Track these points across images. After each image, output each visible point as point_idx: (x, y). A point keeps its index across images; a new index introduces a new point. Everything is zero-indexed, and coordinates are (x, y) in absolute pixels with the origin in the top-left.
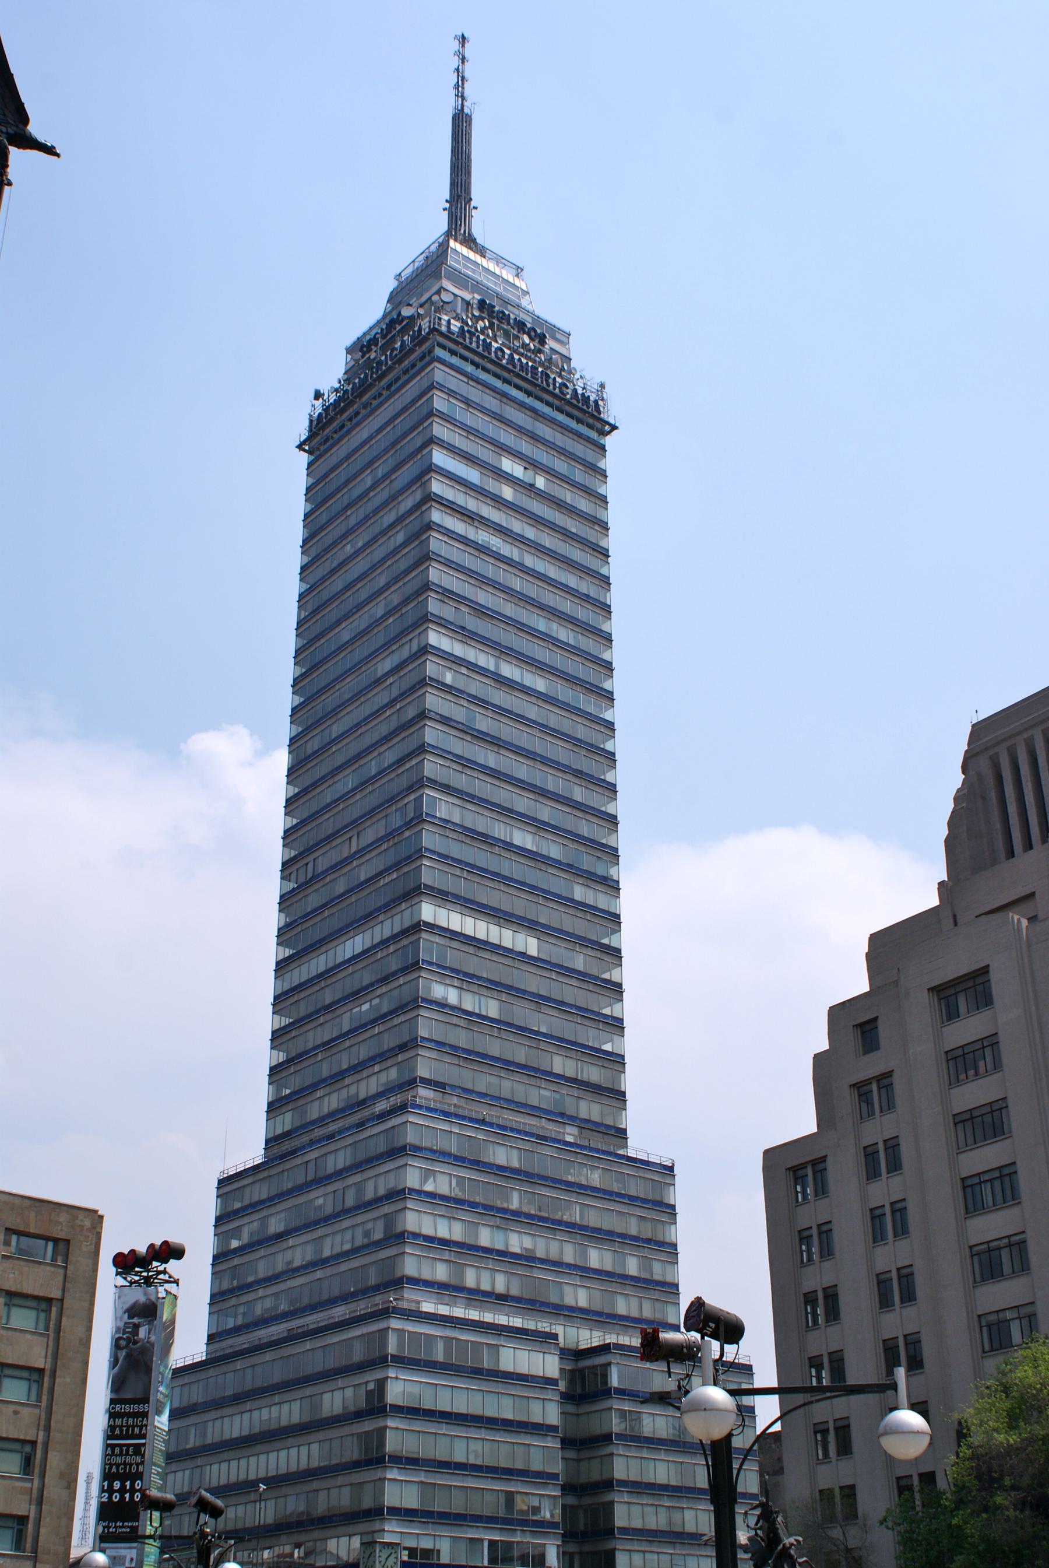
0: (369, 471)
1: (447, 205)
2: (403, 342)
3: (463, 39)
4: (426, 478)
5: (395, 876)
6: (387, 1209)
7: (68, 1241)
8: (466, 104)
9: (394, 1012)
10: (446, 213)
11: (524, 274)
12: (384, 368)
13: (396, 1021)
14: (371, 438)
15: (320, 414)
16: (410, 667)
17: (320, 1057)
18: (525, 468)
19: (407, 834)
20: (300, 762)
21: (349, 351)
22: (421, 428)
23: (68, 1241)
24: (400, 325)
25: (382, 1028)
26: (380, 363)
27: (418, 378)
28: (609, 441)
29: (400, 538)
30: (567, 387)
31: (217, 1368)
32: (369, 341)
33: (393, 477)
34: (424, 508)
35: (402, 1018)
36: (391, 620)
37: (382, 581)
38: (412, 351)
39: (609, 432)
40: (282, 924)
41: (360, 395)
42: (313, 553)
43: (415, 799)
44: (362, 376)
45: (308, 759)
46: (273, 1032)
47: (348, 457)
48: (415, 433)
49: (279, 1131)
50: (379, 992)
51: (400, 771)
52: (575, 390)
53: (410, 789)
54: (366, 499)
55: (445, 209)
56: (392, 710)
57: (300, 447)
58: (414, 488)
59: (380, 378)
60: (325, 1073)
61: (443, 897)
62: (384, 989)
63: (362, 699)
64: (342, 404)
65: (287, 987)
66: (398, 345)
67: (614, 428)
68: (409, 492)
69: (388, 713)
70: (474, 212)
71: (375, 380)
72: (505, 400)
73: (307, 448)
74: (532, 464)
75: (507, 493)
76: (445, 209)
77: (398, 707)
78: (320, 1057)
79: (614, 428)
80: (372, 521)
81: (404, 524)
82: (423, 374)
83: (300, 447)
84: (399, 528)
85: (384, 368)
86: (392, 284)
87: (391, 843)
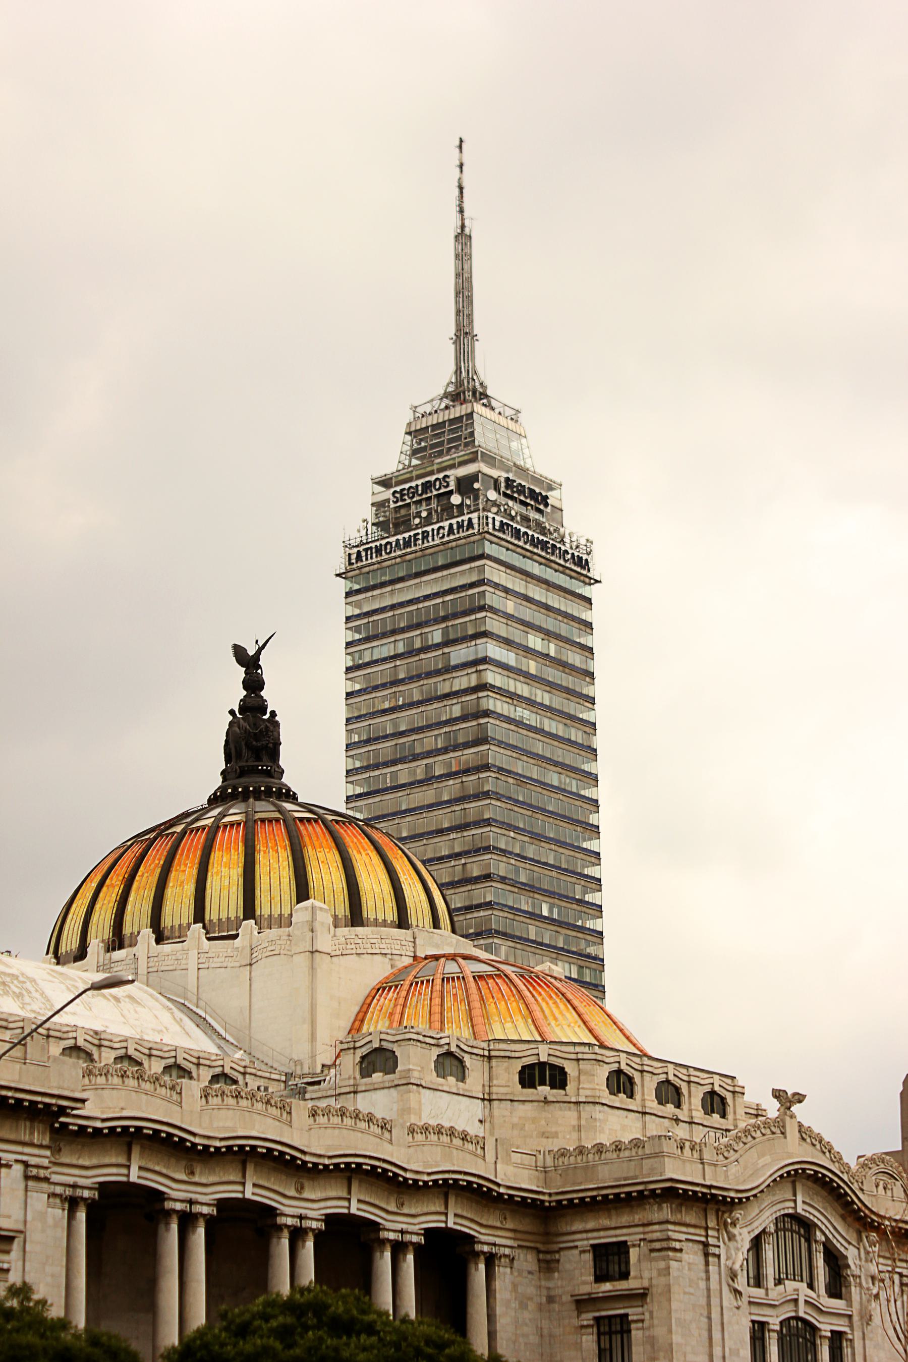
8: (467, 223)
11: (522, 418)
18: (543, 640)
29: (457, 711)
30: (568, 553)
33: (446, 650)
36: (451, 782)
39: (593, 584)
47: (393, 607)
48: (467, 619)
51: (469, 916)
52: (573, 554)
56: (457, 863)
58: (470, 671)
68: (465, 672)
70: (476, 343)
72: (529, 579)
74: (548, 634)
75: (532, 667)
77: (463, 861)
81: (460, 701)
83: (337, 575)
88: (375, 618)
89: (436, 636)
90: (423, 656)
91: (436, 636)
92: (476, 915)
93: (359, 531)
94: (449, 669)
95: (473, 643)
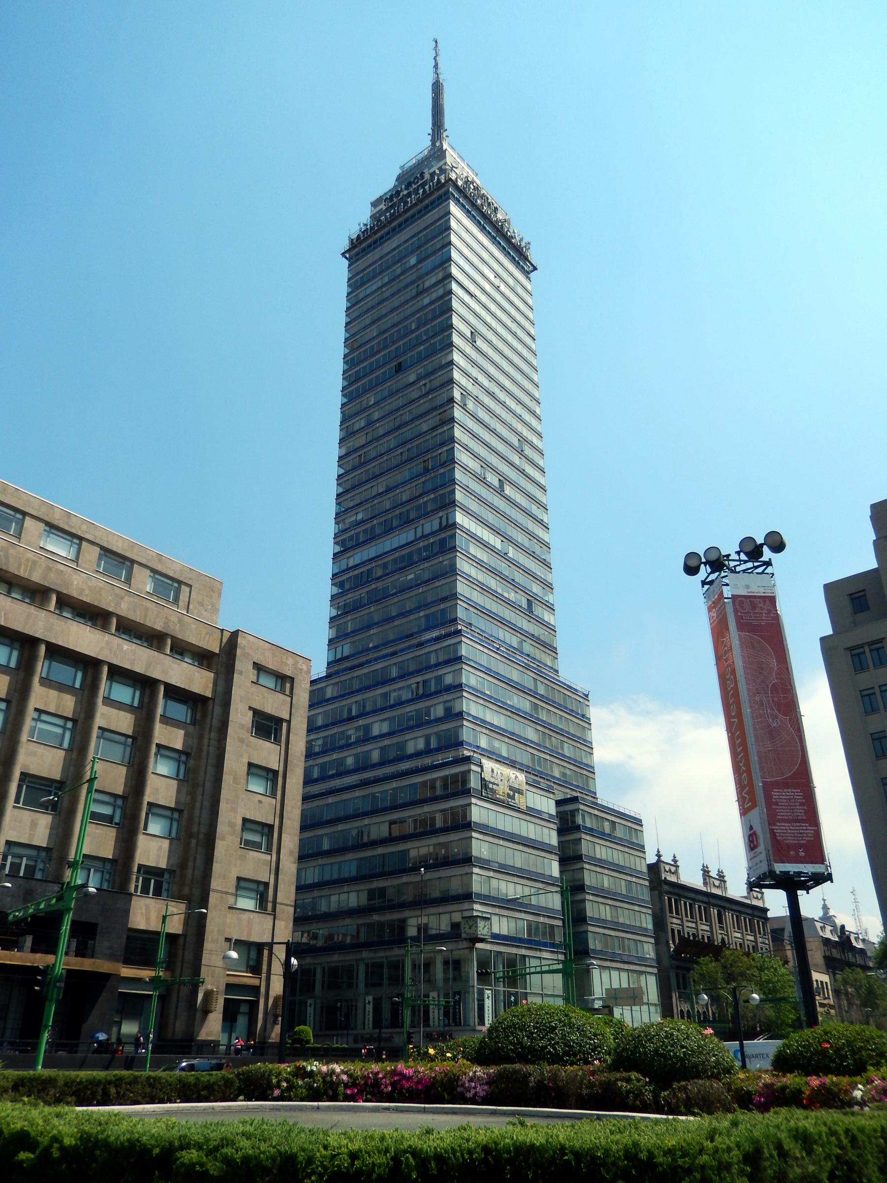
0: (399, 264)
1: (430, 132)
2: (424, 191)
3: (436, 42)
4: (446, 265)
5: (432, 496)
6: (446, 697)
7: (292, 680)
9: (435, 578)
10: (430, 137)
12: (409, 205)
13: (437, 584)
14: (399, 246)
15: (358, 235)
16: (439, 374)
17: (372, 609)
19: (442, 471)
20: (351, 434)
21: (374, 204)
22: (441, 237)
23: (292, 680)
24: (415, 184)
25: (425, 589)
26: (406, 203)
27: (437, 209)
28: (532, 275)
31: (310, 803)
32: (391, 196)
33: (419, 266)
34: (446, 282)
35: (443, 582)
37: (413, 327)
38: (431, 193)
40: (337, 531)
41: (390, 223)
42: (354, 315)
43: (447, 450)
44: (392, 211)
45: (354, 433)
46: (332, 596)
47: (381, 258)
49: (339, 656)
50: (422, 567)
51: (434, 434)
53: (442, 444)
54: (398, 281)
55: (429, 134)
56: (425, 400)
57: (343, 254)
58: (437, 271)
59: (405, 212)
60: (376, 618)
61: (467, 512)
62: (426, 565)
63: (400, 395)
64: (376, 228)
65: (344, 567)
66: (421, 191)
67: (535, 269)
68: (434, 273)
69: (422, 401)
71: (403, 212)
73: (348, 256)
76: (429, 134)
77: (430, 397)
78: (372, 609)
79: (535, 269)
80: (403, 292)
82: (440, 207)
83: (343, 254)
84: (425, 295)
85: (409, 205)
86: (399, 171)
87: (428, 477)
88: (368, 270)
89: (413, 260)
90: (402, 277)
91: (413, 260)
92: (440, 431)
93: (359, 225)
94: (420, 278)
95: (440, 253)
